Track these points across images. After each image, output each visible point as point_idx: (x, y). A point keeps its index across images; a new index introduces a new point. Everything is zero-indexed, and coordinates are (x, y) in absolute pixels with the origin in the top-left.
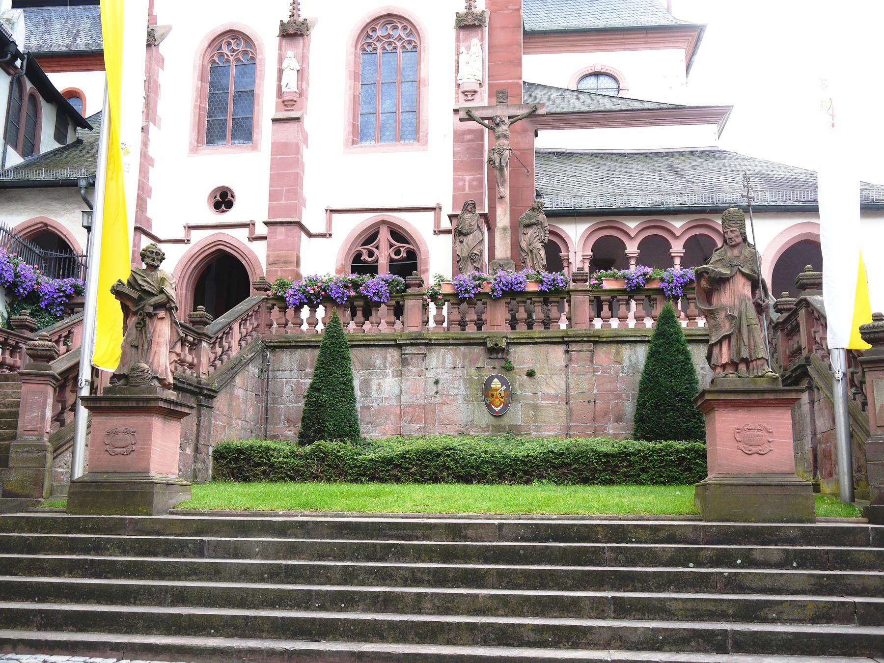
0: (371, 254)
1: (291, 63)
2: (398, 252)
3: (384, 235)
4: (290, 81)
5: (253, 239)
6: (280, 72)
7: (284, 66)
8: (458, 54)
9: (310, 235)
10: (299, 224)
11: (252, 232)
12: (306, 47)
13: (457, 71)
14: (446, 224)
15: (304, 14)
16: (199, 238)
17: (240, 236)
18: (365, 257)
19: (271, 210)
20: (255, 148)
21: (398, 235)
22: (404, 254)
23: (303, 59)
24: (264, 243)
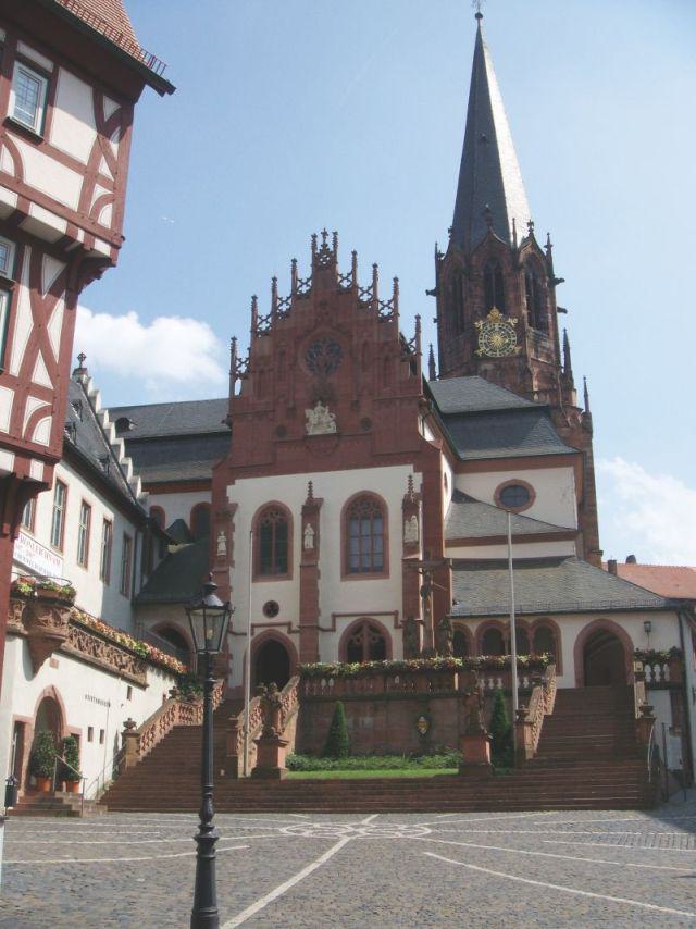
0: (358, 640)
1: (309, 530)
2: (374, 639)
3: (366, 629)
4: (309, 542)
5: (290, 631)
6: (303, 536)
7: (307, 531)
8: (404, 524)
9: (323, 630)
10: (318, 628)
11: (290, 629)
12: (317, 521)
13: (404, 534)
14: (400, 623)
15: (316, 495)
16: (258, 631)
17: (284, 630)
18: (356, 643)
19: (302, 620)
20: (290, 578)
21: (376, 629)
22: (377, 641)
23: (316, 528)
24: (298, 635)
